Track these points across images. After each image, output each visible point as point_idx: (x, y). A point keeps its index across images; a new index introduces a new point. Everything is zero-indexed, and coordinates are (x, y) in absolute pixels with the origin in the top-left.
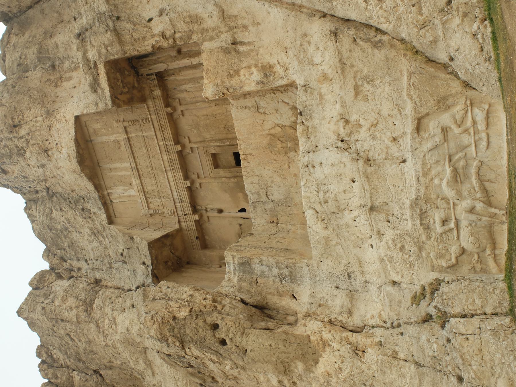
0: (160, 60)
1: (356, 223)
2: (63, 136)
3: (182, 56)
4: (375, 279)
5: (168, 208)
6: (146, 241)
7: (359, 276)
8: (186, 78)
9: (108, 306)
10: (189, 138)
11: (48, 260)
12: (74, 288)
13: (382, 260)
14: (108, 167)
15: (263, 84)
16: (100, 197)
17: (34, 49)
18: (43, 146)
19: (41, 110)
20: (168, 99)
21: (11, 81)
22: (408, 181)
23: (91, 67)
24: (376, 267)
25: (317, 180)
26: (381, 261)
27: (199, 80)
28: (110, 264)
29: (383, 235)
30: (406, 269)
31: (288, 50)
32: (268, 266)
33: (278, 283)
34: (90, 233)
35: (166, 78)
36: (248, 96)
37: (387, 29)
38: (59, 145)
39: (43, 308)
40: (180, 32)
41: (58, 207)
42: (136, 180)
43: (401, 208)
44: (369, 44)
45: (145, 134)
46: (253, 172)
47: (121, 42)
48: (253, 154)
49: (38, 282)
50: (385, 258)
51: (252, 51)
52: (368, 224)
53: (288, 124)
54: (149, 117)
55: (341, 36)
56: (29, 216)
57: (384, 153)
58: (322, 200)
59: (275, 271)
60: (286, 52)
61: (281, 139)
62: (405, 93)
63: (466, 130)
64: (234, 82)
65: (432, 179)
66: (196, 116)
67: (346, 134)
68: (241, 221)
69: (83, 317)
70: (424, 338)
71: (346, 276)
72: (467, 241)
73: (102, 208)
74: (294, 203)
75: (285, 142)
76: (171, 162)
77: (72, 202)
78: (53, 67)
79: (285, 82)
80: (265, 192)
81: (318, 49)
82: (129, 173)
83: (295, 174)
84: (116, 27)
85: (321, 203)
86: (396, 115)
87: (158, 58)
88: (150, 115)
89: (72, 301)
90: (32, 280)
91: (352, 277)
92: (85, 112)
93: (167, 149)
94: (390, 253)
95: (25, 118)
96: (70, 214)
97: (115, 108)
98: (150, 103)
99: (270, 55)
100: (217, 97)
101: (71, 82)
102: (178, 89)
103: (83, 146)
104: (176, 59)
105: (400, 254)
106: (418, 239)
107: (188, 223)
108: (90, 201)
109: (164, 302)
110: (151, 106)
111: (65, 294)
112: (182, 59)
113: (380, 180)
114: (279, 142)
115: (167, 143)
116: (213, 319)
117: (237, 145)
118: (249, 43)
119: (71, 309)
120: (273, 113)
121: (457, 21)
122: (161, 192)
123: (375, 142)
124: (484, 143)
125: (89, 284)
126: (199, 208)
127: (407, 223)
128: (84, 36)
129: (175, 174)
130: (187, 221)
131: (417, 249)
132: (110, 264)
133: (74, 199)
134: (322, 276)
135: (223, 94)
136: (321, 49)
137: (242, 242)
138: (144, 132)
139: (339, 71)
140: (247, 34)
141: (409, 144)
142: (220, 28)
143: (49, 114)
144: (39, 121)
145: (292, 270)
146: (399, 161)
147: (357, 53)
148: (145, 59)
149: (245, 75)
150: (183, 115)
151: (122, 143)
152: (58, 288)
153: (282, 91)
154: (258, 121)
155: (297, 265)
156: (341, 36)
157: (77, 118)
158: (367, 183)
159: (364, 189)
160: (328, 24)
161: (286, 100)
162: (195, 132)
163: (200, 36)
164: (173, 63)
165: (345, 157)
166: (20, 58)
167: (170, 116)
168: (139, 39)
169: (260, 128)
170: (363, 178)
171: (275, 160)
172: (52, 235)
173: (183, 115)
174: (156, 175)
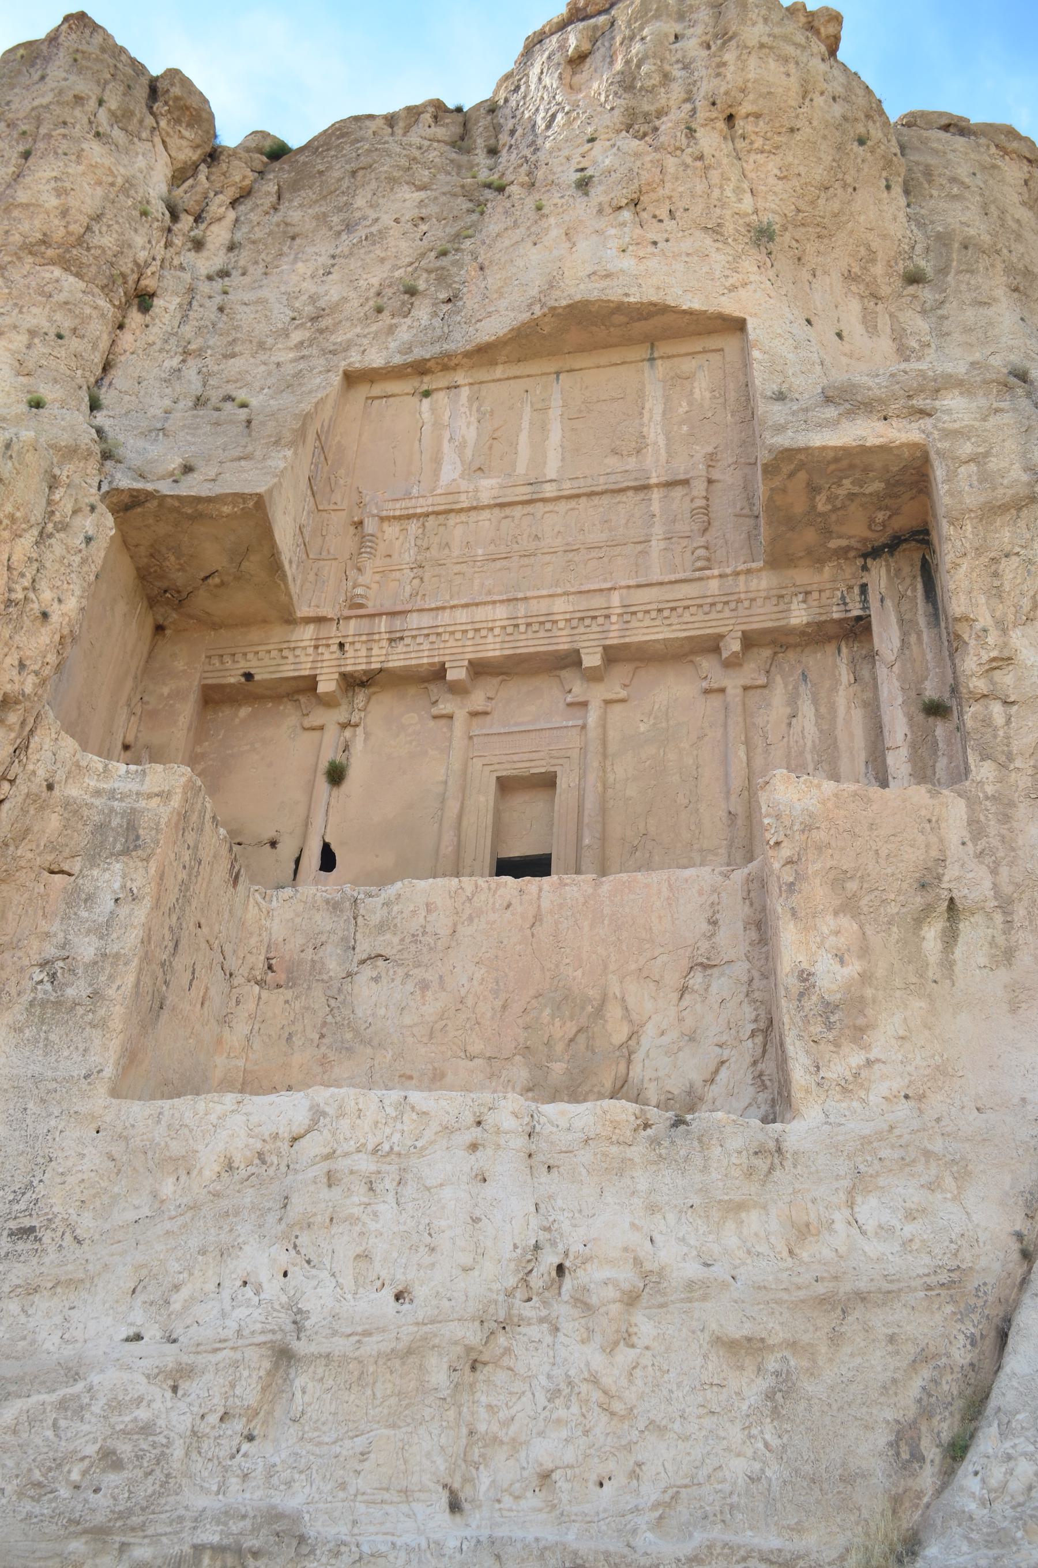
0: (913, 639)
3: (920, 717)
5: (375, 586)
6: (270, 491)
8: (840, 721)
9: (50, 320)
10: (623, 701)
11: (245, 147)
12: (136, 213)
14: (553, 404)
15: (801, 995)
16: (449, 356)
17: (978, 229)
18: (653, 196)
19: (774, 212)
20: (771, 643)
21: (880, 135)
23: (917, 400)
24: (48, 1345)
25: (421, 1152)
26: (69, 1369)
27: (826, 767)
28: (200, 353)
29: (175, 1389)
30: (25, 1466)
31: (912, 1103)
32: (108, 924)
33: (37, 949)
34: (322, 303)
35: (844, 650)
36: (754, 935)
37: (961, 1489)
38: (651, 249)
39: (79, 99)
40: (1008, 722)
41: (432, 209)
43: (271, 1471)
44: (911, 1414)
45: (656, 545)
46: (471, 919)
47: (992, 511)
48: (537, 929)
49: (177, 99)
50: (80, 1386)
53: (636, 1071)
54: (716, 572)
55: (949, 1309)
56: (413, 113)
57: (495, 1428)
58: (341, 1164)
59: (87, 949)
60: (906, 1097)
61: (582, 1039)
62: (716, 1533)
64: (817, 892)
66: (700, 738)
67: (585, 1289)
68: (287, 850)
69: (25, 227)
71: (27, 1223)
73: (410, 359)
74: (331, 1055)
75: (570, 1053)
76: (548, 621)
77: (445, 261)
78: (914, 279)
79: (799, 1075)
81: (910, 1216)
82: (521, 469)
83: (443, 1075)
85: (330, 1156)
86: (637, 1492)
87: (919, 634)
88: (720, 576)
89: (88, 200)
90: (186, 83)
91: (20, 1246)
92: (756, 354)
93: (594, 618)
94: (96, 1409)
95: (753, 157)
96: (403, 247)
97: (764, 456)
98: (764, 582)
99: (901, 1033)
100: (766, 821)
101: (859, 329)
102: (802, 688)
103: (639, 327)
104: (913, 694)
105: (91, 1450)
106: (143, 1527)
107: (311, 650)
108: (437, 322)
109: (37, 514)
110: (754, 584)
111: (120, 181)
112: (911, 719)
113: (393, 1401)
114: (571, 1028)
115: (614, 619)
117: (578, 871)
118: (948, 965)
119: (60, 192)
120: (681, 1020)
123: (541, 1399)
125: (140, 269)
127: (208, 1492)
128: (1020, 391)
129: (497, 631)
130: (316, 647)
131: (99, 1518)
132: (200, 353)
133: (454, 270)
134: (42, 1129)
135: (778, 844)
136: (909, 1229)
137: (213, 841)
139: (821, 1289)
140: (982, 961)
141: (518, 1534)
142: (1011, 864)
143: (763, 236)
144: (740, 200)
145: (80, 1011)
146: (456, 1485)
148: (920, 586)
149: (837, 933)
150: (707, 692)
151: (632, 463)
152: (141, 162)
153: (760, 1066)
154: (659, 961)
155: (96, 1033)
156: (949, 1309)
157: (738, 326)
158: (386, 1347)
159: (367, 1333)
160: (997, 1266)
161: (724, 1074)
162: (643, 728)
163: (990, 789)
164: (897, 684)
165: (495, 1275)
166: (954, 180)
167: (712, 645)
168: (996, 575)
169: (633, 967)
171: (504, 1007)
172: (336, 174)
173: (707, 692)
174: (504, 563)
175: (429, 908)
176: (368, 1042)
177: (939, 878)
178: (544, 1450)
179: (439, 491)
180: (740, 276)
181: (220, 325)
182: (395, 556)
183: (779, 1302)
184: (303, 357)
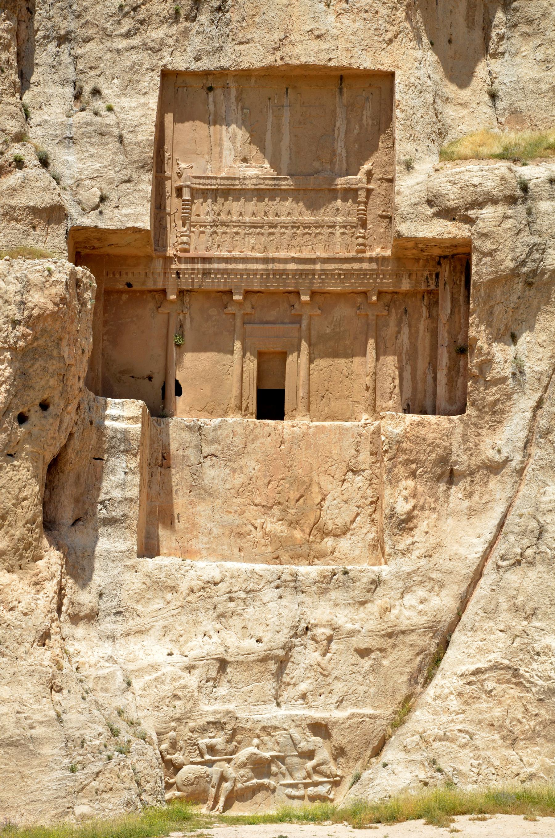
1: (200, 637)
2: (359, 24)
3: (454, 354)
4: (121, 653)
7: (120, 628)
8: (420, 338)
13: (155, 667)
22: (257, 708)
35: (426, 298)
42: (255, 181)
43: (223, 697)
45: (338, 231)
46: (253, 440)
47: (492, 283)
48: (282, 447)
51: (437, 500)
52: (203, 655)
58: (234, 595)
59: (117, 494)
61: (302, 500)
63: (309, 776)
65: (258, 737)
66: (356, 338)
68: (157, 381)
70: (101, 730)
71: (120, 610)
72: (188, 772)
76: (284, 272)
80: (217, 453)
81: (422, 602)
83: (244, 512)
84: (517, 279)
85: (230, 592)
92: (397, 113)
94: (168, 680)
100: (383, 438)
102: (404, 317)
105: (170, 694)
116: (56, 400)
121: (422, 776)
122: (224, 229)
123: (302, 670)
124: (294, 792)
126: (187, 299)
131: (178, 716)
134: (116, 572)
138: (342, 230)
139: (390, 630)
147: (407, 654)
148: (463, 279)
153: (373, 516)
160: (448, 620)
161: (358, 518)
163: (473, 420)
164: (446, 335)
169: (323, 469)
170: (262, 654)
175: (234, 433)
176: (211, 495)
177: (448, 461)
178: (303, 687)
179: (223, 175)
180: (395, 28)
181: (74, 7)
182: (202, 216)
183: (376, 635)
184: (133, 47)
